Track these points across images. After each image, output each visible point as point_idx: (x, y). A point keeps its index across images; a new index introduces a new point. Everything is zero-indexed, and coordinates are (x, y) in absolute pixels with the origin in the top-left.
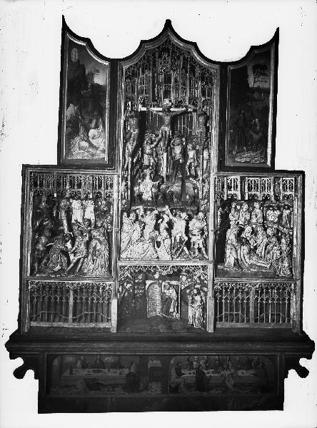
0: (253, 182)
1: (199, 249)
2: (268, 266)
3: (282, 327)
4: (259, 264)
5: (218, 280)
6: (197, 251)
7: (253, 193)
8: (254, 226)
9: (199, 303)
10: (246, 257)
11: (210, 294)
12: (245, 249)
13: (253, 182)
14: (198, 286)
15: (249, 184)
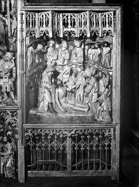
0: (69, 18)
1: (8, 94)
2: (86, 110)
3: (101, 175)
4: (76, 108)
5: (26, 126)
6: (6, 94)
7: (69, 30)
8: (74, 66)
9: (9, 152)
10: (62, 101)
11: (19, 142)
12: (60, 91)
13: (69, 18)
14: (9, 133)
15: (64, 20)
